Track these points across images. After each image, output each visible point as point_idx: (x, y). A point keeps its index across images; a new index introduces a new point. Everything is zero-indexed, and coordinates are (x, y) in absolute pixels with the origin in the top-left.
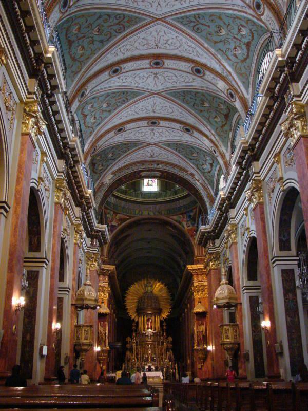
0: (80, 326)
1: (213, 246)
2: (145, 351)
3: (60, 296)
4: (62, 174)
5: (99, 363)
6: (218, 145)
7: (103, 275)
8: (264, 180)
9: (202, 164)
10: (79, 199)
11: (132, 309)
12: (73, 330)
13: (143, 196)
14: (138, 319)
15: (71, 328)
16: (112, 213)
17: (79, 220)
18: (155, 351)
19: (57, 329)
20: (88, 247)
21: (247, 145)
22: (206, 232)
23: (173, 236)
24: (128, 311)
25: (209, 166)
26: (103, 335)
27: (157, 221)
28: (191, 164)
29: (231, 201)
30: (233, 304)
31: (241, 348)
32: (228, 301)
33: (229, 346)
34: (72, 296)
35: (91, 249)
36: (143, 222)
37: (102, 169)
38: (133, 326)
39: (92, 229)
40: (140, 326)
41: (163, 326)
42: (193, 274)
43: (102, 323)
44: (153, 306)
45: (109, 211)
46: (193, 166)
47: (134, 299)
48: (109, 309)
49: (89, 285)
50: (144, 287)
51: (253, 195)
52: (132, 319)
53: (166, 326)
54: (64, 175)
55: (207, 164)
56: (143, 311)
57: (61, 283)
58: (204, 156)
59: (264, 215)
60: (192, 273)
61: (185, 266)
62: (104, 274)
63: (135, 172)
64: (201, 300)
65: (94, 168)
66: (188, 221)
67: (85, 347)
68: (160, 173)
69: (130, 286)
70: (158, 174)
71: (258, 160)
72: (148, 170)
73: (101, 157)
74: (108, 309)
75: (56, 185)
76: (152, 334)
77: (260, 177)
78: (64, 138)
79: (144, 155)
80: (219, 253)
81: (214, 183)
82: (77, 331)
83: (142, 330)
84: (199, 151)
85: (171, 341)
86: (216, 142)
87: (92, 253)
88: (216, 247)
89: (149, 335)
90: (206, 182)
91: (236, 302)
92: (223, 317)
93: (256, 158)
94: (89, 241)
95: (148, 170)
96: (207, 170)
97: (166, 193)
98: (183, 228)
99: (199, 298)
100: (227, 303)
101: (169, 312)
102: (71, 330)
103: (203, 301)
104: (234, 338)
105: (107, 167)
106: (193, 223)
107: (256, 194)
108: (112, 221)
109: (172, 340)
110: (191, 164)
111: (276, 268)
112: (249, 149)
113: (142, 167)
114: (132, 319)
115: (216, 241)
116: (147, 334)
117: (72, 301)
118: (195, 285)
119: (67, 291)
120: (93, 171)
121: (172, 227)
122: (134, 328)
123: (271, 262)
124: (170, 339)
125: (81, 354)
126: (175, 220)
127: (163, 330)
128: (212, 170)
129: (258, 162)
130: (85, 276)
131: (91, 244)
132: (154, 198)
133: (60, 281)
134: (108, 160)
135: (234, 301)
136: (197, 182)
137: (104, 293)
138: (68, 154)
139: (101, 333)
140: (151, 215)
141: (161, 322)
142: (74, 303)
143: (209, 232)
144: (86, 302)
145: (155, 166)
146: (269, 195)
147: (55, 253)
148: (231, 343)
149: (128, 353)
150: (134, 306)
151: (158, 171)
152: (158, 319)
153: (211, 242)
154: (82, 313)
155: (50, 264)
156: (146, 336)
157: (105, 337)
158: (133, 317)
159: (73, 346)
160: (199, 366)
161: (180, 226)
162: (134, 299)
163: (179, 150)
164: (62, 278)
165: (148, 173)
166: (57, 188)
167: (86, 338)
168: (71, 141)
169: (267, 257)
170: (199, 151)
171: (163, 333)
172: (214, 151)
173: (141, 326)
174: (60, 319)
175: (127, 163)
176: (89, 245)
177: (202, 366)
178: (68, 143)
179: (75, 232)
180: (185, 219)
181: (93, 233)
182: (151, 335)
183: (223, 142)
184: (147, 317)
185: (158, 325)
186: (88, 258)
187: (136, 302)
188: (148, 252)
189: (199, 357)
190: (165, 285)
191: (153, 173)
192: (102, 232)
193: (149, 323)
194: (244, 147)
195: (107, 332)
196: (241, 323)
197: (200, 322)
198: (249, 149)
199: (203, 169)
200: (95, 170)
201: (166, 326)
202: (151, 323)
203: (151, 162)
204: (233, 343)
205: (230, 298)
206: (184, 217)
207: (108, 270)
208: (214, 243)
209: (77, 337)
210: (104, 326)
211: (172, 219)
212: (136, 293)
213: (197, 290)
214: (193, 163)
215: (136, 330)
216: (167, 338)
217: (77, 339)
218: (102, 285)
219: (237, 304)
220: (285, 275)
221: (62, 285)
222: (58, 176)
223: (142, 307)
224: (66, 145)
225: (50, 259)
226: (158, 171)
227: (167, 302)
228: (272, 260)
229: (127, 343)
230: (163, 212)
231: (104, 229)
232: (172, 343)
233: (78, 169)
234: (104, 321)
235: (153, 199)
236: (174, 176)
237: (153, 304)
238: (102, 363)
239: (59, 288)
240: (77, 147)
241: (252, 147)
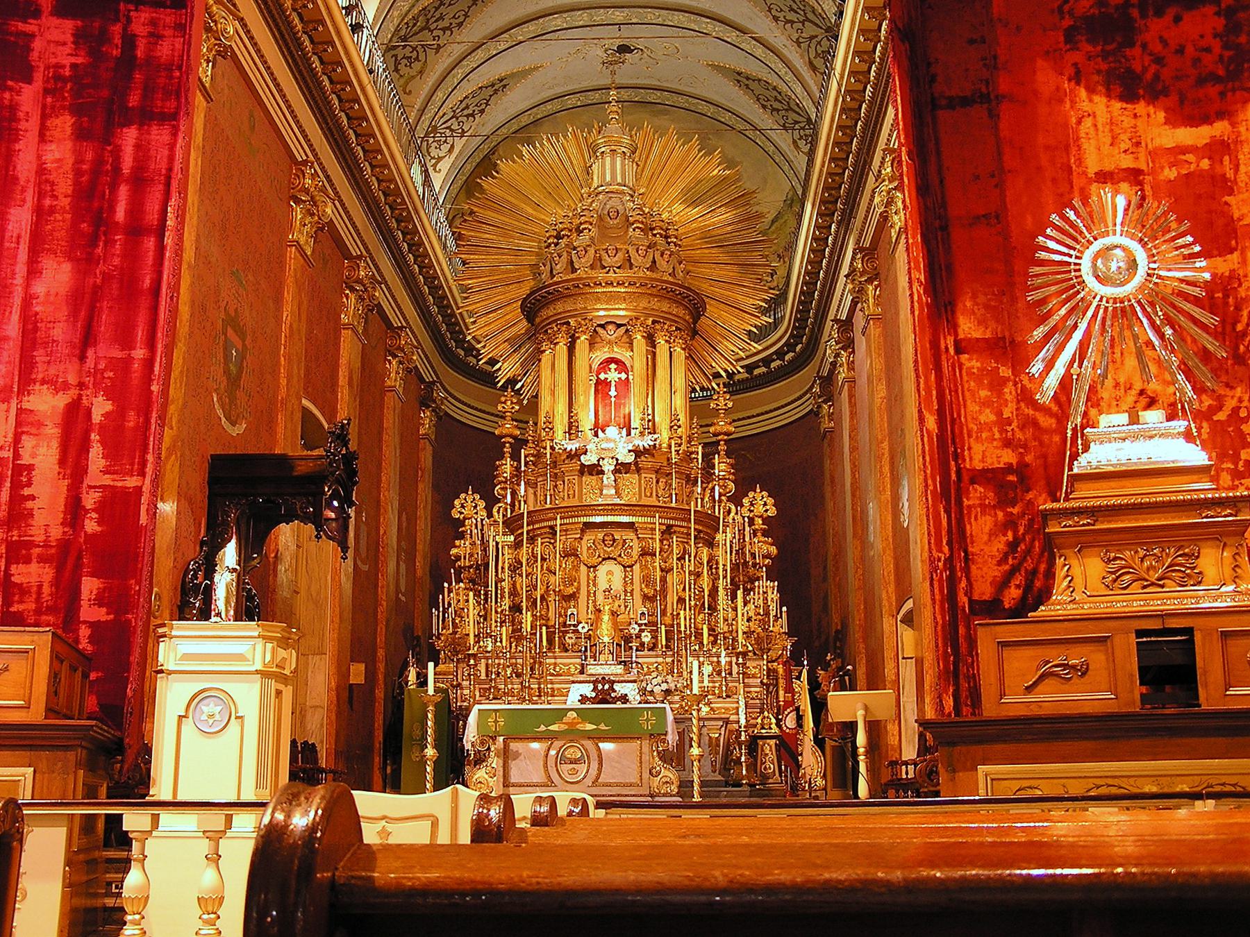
2: (572, 580)
18: (647, 580)
56: (559, 307)
76: (630, 458)
85: (766, 520)
89: (608, 466)
109: (772, 512)
124: (762, 503)
149: (458, 596)
171: (708, 465)
173: (554, 407)
182: (621, 468)
184: (592, 345)
216: (737, 500)
229: (455, 529)
232: (772, 528)
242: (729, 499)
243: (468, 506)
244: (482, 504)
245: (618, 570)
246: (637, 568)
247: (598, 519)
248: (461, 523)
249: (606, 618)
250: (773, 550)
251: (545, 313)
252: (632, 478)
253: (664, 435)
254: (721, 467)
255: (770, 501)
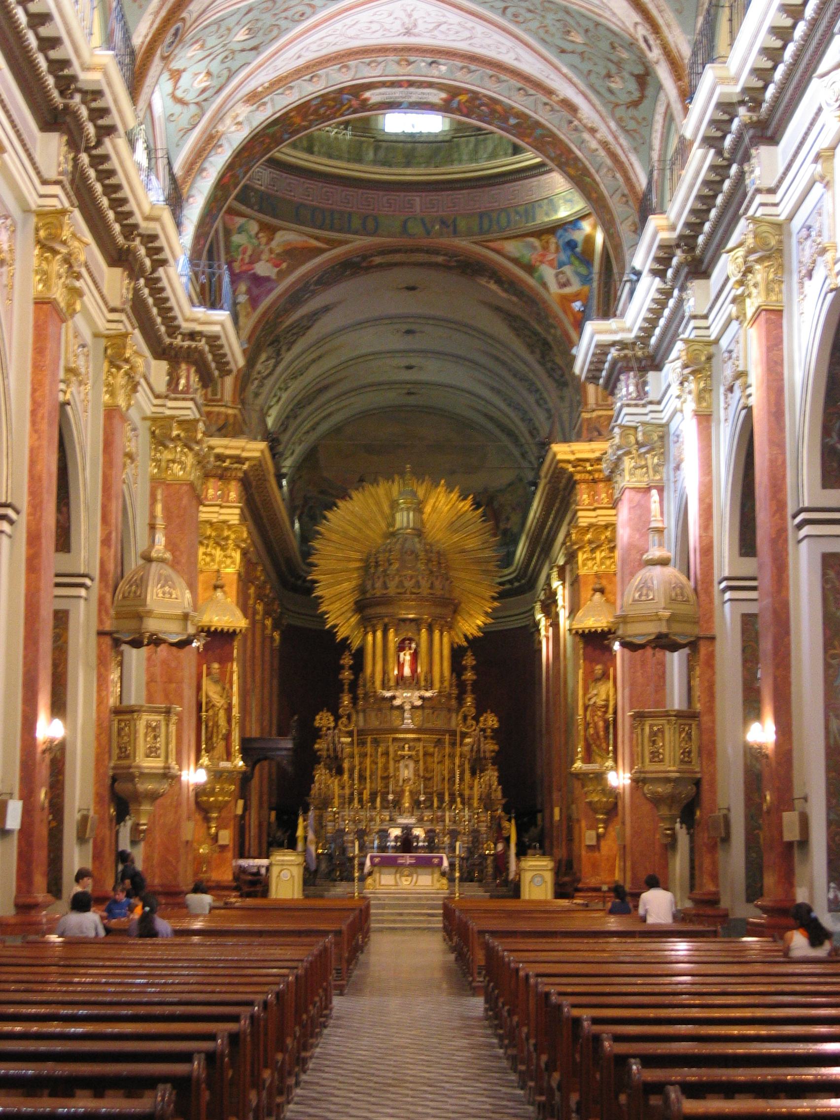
0: (131, 711)
1: (639, 397)
2: (386, 768)
3: (62, 605)
4: (56, 190)
5: (207, 820)
6: (661, 21)
7: (221, 477)
8: (790, 218)
9: (604, 72)
10: (121, 240)
11: (339, 597)
12: (106, 724)
13: (381, 154)
14: (364, 639)
15: (99, 718)
16: (254, 227)
17: (123, 317)
19: (52, 741)
20: (157, 397)
21: (738, 89)
22: (614, 344)
23: (510, 318)
24: (323, 608)
25: (633, 86)
26: (222, 713)
27: (440, 259)
28: (565, 70)
29: (698, 251)
30: (683, 641)
31: (706, 796)
32: (664, 629)
33: (660, 790)
34: (101, 602)
35: (170, 404)
36: (378, 260)
37: (204, 91)
38: (342, 667)
39: (173, 330)
40: (369, 670)
41: (465, 668)
42: (578, 477)
43: (216, 666)
44: (425, 591)
45: (240, 221)
46: (570, 74)
47: (349, 560)
48: (246, 616)
49: (162, 560)
50: (387, 510)
51: (749, 270)
52: (340, 637)
53: (473, 668)
54: (63, 187)
55: (625, 74)
57: (62, 556)
58: (614, 48)
59: (781, 350)
60: (571, 475)
61: (544, 446)
62: (223, 476)
63: (341, 91)
64: (604, 582)
65: (175, 88)
66: (561, 264)
67: (150, 786)
68: (444, 95)
69: (331, 506)
70: (436, 96)
71: (773, 140)
72: (393, 84)
73: (202, 47)
74: (238, 613)
75: (37, 230)
76: (419, 703)
77: (776, 205)
78: (59, 66)
79: (375, 27)
80: (662, 426)
81: (651, 148)
82: (120, 730)
83: (378, 683)
84: (591, 26)
85: (493, 730)
86: (654, 12)
87: (172, 418)
88: (651, 403)
89: (407, 707)
90: (622, 140)
91: (696, 631)
92: (664, 673)
93: (769, 133)
94: (159, 370)
95: (393, 84)
96: (624, 98)
97: (476, 145)
98: (541, 290)
99: (597, 576)
100: (660, 636)
101: (487, 614)
102: (99, 725)
103: (608, 588)
104: (682, 762)
105: (229, 78)
106: (583, 270)
107: (760, 274)
108: (255, 258)
110: (565, 70)
111: (804, 544)
112: (742, 103)
113: (367, 73)
114: (340, 637)
115: (651, 376)
116: (397, 702)
117: (101, 621)
118: (583, 522)
119: (82, 585)
120: (173, 96)
121: (499, 282)
122: (347, 675)
123: (791, 523)
124: (491, 721)
125: (132, 807)
126: (516, 261)
127: (461, 686)
128: (642, 98)
129: (772, 148)
130: (147, 528)
131: (169, 384)
132: (428, 164)
133: (57, 550)
134: (233, 52)
135: (688, 628)
136: (586, 136)
137: (224, 548)
138: (75, 115)
139: (210, 705)
140: (411, 236)
141: (457, 653)
142: (108, 627)
143: (623, 345)
144: (152, 625)
145: (421, 69)
146: (801, 284)
147: (40, 479)
148: (668, 780)
149: (321, 776)
150: (346, 585)
151: (430, 85)
152: (443, 644)
153: (632, 381)
154: (135, 657)
155: (22, 520)
156: (393, 708)
157: (229, 721)
158: (342, 633)
159: (108, 781)
160: (589, 837)
161: (531, 281)
162: (349, 560)
163: (515, 15)
164: (64, 542)
165: (396, 94)
166: (38, 242)
167: (152, 752)
168: (86, 68)
169: (781, 506)
170: (591, 26)
172: (646, 41)
173: (373, 668)
174: (59, 708)
175: (309, 56)
176: (161, 387)
177: (599, 837)
178: (73, 78)
179: (106, 365)
180: (551, 257)
181: (178, 341)
182: (414, 707)
183: (679, 12)
184: (396, 631)
185: (442, 668)
186: (160, 440)
187: (358, 569)
188: (409, 368)
189: (590, 803)
190: (477, 505)
191: (416, 94)
192: (213, 340)
193: (406, 657)
194: (721, 94)
195: (235, 700)
196: (711, 710)
197: (599, 668)
198: (742, 103)
199: (611, 91)
200: (179, 94)
201: (473, 668)
202: (415, 656)
203: (405, 52)
204: (676, 780)
205: (671, 620)
206: (546, 248)
207: (239, 460)
208: (641, 386)
209: (122, 749)
210: (223, 680)
211: (493, 250)
212: (353, 532)
213: (590, 542)
214: (573, 67)
215: (354, 686)
216: (476, 719)
217: (119, 758)
218: (214, 518)
219: (699, 638)
220: (832, 574)
221: (63, 562)
222: (41, 196)
223: (378, 593)
224: (66, 84)
225: (23, 503)
226: (430, 85)
227: (486, 572)
228: (794, 517)
230: (462, 224)
231: (217, 329)
232: (497, 735)
233: (115, 147)
234: (225, 659)
235: (422, 171)
236: (498, 107)
237: (425, 584)
238: (217, 818)
239: (58, 575)
240: (110, 84)
241: (753, 97)
242: (473, 718)
243: (323, 720)
244: (332, 718)
245: (412, 765)
246: (421, 763)
247: (401, 736)
248: (320, 729)
249: (407, 794)
250: (496, 747)
251: (370, 611)
252: (419, 712)
253: (437, 684)
254: (469, 700)
255: (496, 719)
